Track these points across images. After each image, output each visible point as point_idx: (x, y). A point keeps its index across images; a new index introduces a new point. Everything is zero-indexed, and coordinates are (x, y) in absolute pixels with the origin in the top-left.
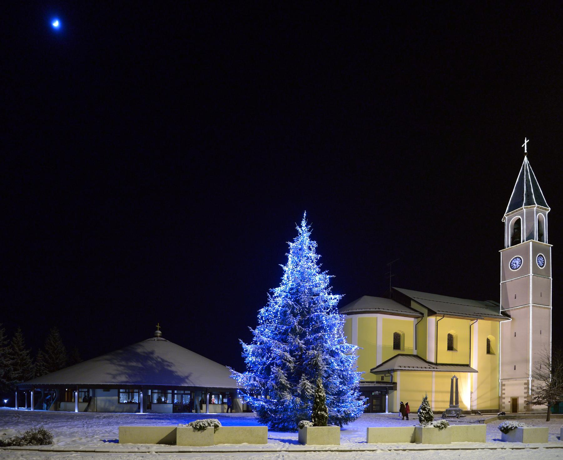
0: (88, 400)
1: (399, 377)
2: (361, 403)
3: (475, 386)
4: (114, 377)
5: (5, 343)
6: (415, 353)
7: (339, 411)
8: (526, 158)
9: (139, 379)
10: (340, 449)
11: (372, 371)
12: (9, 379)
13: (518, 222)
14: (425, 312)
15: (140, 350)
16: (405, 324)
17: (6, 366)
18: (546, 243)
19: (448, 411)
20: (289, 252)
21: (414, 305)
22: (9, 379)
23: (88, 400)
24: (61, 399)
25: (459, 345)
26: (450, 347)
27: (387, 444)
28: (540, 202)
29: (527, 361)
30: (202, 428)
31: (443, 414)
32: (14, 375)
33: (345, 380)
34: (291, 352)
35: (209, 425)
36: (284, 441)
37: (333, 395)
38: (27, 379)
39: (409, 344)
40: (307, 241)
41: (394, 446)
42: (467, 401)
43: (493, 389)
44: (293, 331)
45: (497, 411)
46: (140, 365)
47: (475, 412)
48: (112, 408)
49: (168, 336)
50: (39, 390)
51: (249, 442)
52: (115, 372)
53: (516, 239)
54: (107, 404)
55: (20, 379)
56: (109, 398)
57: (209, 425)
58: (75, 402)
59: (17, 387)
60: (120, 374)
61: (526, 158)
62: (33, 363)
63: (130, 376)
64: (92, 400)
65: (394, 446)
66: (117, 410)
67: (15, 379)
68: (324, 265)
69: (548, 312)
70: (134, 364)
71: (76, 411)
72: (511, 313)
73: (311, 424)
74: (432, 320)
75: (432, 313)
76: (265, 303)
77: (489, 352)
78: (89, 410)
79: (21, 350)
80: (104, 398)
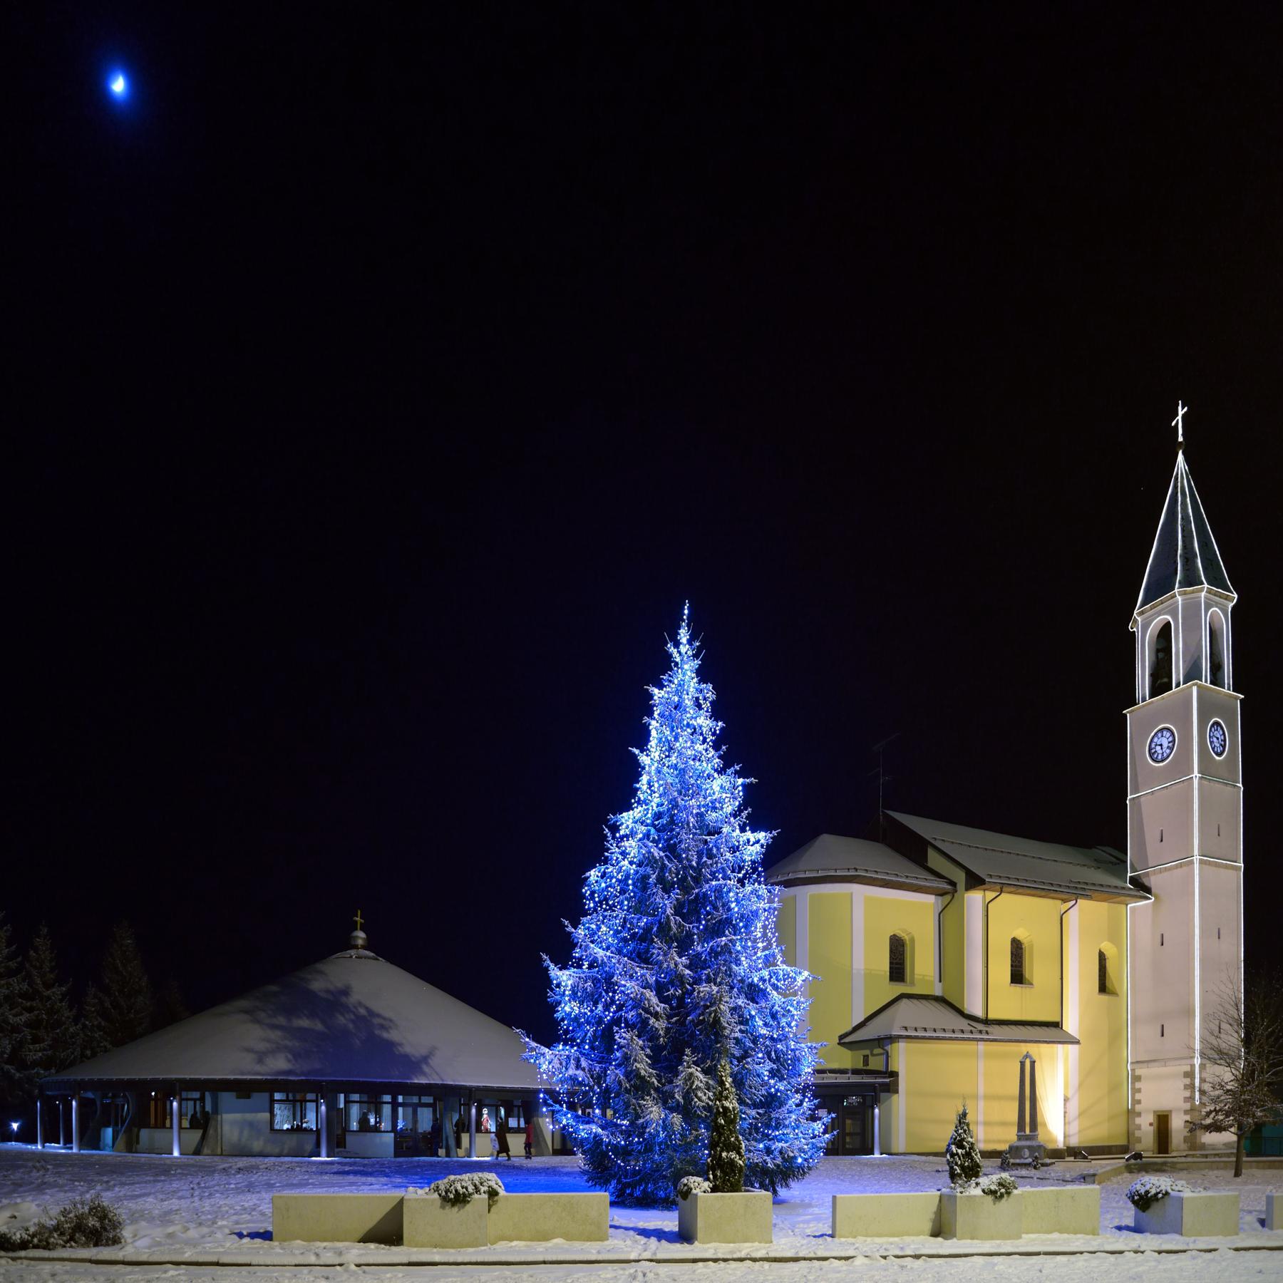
0: (202, 1122)
1: (904, 1058)
2: (818, 1127)
3: (1074, 1081)
4: (261, 1057)
5: (12, 965)
6: (937, 991)
7: (768, 1151)
8: (1180, 457)
10: (772, 1255)
11: (843, 1041)
12: (22, 1065)
13: (1165, 631)
14: (960, 877)
15: (317, 985)
16: (913, 911)
17: (16, 1029)
18: (1227, 690)
19: (1014, 1150)
20: (651, 715)
21: (934, 860)
22: (22, 1065)
23: (202, 1122)
24: (141, 1120)
25: (1037, 969)
26: (1018, 977)
27: (878, 1240)
28: (1215, 580)
29: (1189, 1013)
30: (460, 1199)
31: (1005, 1159)
32: (34, 1053)
33: (783, 1065)
34: (660, 989)
35: (477, 1190)
36: (645, 1233)
37: (755, 1106)
38: (63, 1066)
39: (923, 966)
40: (692, 684)
41: (893, 1244)
42: (1056, 1125)
43: (1114, 1088)
44: (664, 929)
45: (1124, 1149)
46: (319, 1026)
47: (1074, 1152)
48: (257, 1145)
49: (384, 948)
50: (90, 1095)
51: (568, 1237)
52: (262, 1046)
53: (1161, 683)
54: (246, 1133)
55: (47, 1064)
56: (249, 1116)
57: (477, 1190)
58: (171, 1127)
60: (276, 1050)
61: (1180, 457)
62: (76, 1020)
63: (297, 1055)
64: (212, 1123)
65: (893, 1244)
66: (269, 1149)
67: (35, 1064)
68: (734, 748)
69: (1233, 878)
70: (304, 1023)
71: (176, 1153)
72: (1153, 882)
73: (706, 1185)
74: (975, 899)
75: (975, 881)
76: (598, 855)
77: (1103, 988)
78: (206, 1151)
79: (48, 986)
80: (238, 1116)
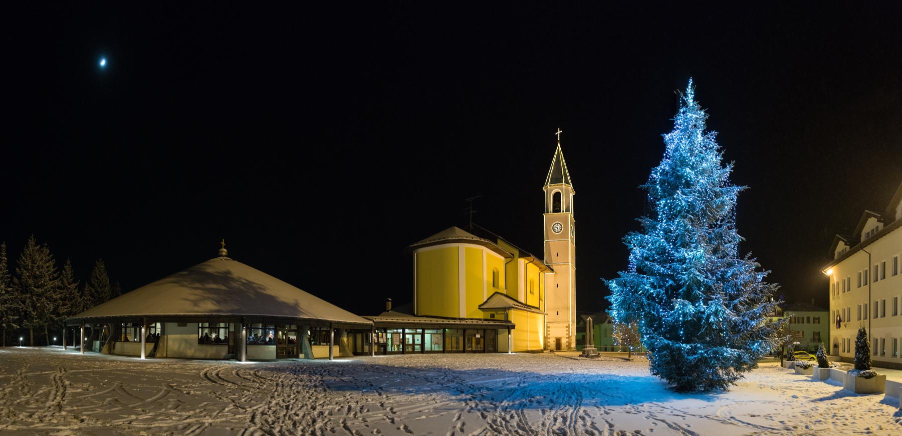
5: (55, 275)
9: (236, 307)
12: (58, 315)
15: (210, 270)
17: (56, 300)
22: (58, 315)
32: (63, 310)
38: (75, 314)
54: (183, 345)
55: (69, 314)
56: (185, 336)
58: (140, 341)
59: (65, 323)
64: (161, 340)
66: (198, 355)
67: (63, 314)
78: (158, 355)
79: (70, 284)
80: (178, 336)
